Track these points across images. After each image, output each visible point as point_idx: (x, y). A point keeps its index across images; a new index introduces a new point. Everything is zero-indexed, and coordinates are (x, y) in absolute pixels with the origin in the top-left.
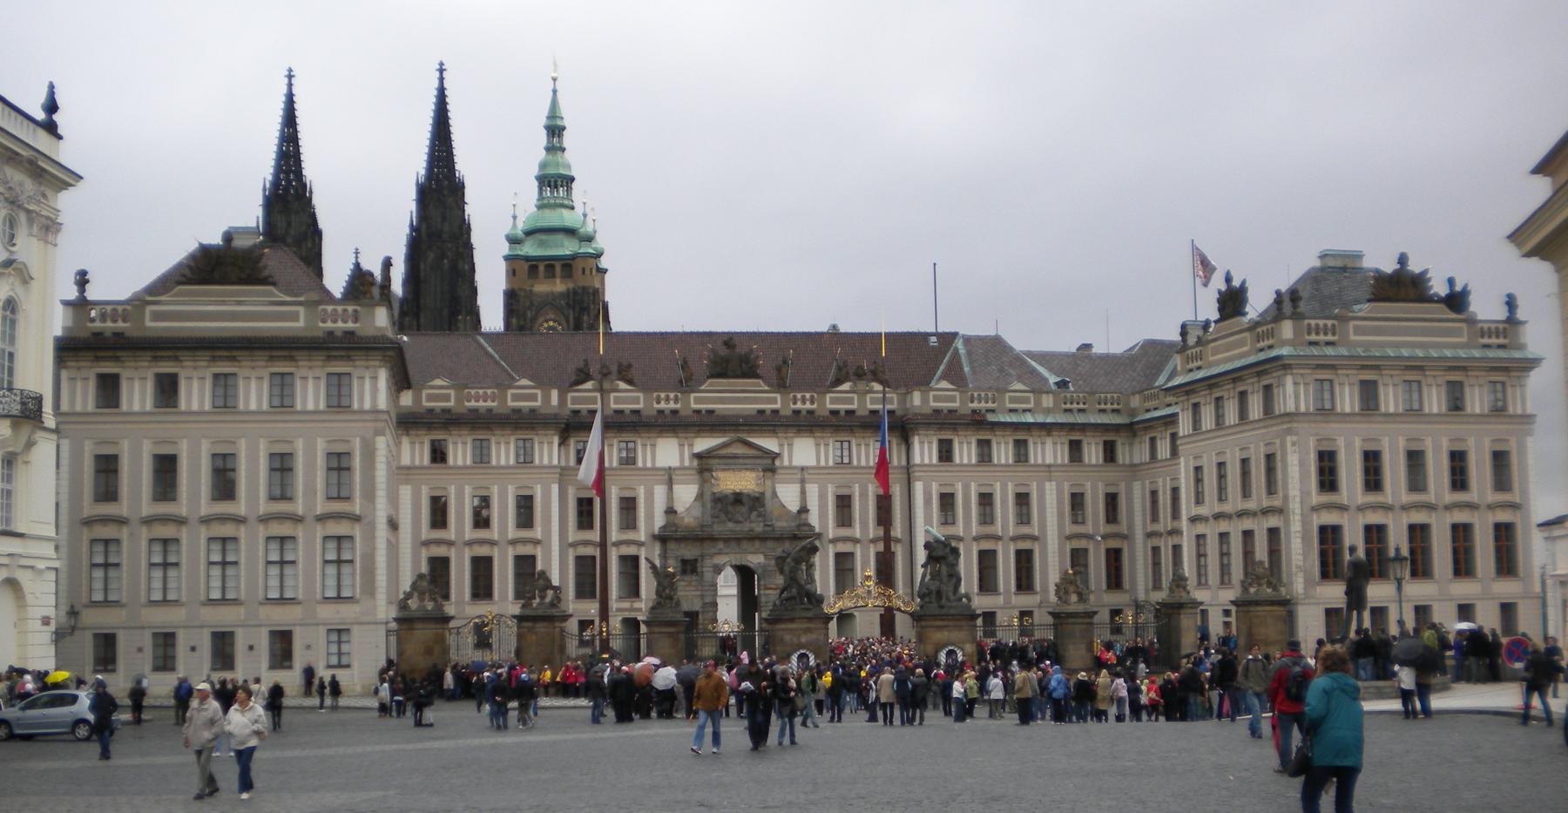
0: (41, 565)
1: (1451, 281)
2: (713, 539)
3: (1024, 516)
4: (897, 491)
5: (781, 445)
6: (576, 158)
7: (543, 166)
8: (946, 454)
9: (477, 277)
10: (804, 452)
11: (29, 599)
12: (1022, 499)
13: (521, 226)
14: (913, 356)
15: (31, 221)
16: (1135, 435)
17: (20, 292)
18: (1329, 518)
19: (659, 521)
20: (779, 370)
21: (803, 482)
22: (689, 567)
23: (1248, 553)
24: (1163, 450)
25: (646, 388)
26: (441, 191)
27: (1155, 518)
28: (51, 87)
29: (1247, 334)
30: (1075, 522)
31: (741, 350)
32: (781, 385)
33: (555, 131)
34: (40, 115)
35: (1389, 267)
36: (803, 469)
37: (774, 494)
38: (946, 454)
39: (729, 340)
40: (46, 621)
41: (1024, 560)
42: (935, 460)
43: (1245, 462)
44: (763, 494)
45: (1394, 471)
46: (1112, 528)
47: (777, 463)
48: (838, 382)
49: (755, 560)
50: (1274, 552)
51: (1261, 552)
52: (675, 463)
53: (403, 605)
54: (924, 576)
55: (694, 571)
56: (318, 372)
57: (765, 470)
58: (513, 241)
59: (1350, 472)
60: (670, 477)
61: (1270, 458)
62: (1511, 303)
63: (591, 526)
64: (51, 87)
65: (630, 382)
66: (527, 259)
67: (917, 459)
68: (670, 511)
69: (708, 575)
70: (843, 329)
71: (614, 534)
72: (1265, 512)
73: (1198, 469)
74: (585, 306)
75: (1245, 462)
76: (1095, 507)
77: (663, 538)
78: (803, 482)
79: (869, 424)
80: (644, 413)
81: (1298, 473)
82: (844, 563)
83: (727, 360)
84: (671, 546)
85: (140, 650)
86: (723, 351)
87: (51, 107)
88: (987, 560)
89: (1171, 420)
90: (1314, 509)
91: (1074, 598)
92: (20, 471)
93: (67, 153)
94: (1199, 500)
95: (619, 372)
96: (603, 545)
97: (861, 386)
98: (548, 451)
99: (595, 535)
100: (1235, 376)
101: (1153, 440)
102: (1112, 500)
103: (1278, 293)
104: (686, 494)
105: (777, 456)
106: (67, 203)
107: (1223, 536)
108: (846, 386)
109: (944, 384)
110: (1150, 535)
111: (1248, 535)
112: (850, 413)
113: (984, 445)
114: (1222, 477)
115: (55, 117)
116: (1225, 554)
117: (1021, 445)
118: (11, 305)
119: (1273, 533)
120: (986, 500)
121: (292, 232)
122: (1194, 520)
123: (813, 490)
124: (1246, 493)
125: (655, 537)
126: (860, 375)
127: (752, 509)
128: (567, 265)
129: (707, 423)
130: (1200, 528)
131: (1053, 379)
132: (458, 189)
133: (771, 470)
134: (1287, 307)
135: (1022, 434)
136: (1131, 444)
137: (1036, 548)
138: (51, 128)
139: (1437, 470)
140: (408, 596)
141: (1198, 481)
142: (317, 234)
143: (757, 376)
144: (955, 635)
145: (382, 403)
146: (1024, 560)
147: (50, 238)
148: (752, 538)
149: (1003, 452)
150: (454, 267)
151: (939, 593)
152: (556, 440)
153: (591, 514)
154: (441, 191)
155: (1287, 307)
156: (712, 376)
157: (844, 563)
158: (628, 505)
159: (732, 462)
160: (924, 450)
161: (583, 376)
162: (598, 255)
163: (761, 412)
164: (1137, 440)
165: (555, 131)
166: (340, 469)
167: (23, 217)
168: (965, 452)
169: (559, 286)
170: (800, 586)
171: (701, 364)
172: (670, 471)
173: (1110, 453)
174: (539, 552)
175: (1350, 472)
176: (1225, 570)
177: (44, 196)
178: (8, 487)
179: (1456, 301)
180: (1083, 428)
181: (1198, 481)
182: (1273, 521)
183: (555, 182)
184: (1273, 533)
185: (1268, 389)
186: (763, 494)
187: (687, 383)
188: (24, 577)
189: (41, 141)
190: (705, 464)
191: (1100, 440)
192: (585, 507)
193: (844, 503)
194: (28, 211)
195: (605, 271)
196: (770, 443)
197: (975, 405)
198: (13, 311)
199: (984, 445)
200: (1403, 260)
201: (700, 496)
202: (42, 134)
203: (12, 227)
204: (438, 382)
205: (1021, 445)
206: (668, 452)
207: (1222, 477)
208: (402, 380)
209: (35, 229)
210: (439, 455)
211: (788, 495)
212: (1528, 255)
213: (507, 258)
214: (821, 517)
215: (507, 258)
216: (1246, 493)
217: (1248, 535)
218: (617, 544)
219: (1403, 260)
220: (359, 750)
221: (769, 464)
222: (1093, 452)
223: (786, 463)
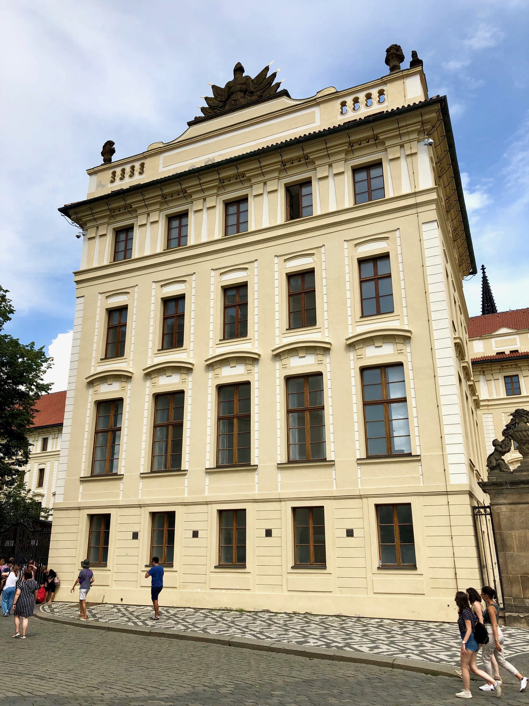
53: (495, 463)
140: (500, 448)
166: (377, 279)
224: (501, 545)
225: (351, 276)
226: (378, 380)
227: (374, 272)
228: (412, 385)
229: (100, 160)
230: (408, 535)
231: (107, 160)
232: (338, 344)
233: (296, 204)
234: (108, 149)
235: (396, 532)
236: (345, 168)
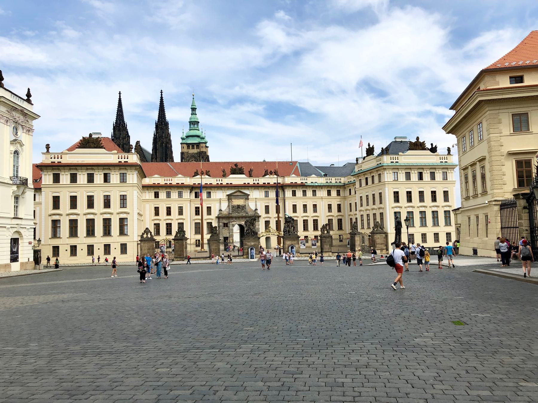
0: (28, 227)
1: (432, 144)
2: (232, 217)
3: (315, 211)
4: (281, 204)
6: (200, 116)
7: (190, 119)
8: (294, 194)
9: (173, 149)
10: (255, 194)
11: (24, 237)
12: (315, 206)
13: (185, 135)
14: (286, 168)
15: (23, 129)
17: (19, 149)
18: (397, 210)
20: (249, 172)
21: (256, 202)
22: (226, 225)
23: (375, 219)
24: (353, 192)
25: (214, 176)
26: (162, 125)
27: (351, 211)
28: (29, 89)
30: (329, 212)
31: (239, 167)
32: (250, 176)
33: (194, 109)
34: (26, 98)
35: (414, 140)
37: (248, 205)
38: (294, 194)
39: (236, 164)
40: (30, 243)
41: (315, 222)
42: (291, 196)
43: (374, 195)
44: (245, 205)
45: (415, 196)
46: (340, 214)
48: (265, 175)
49: (243, 223)
50: (382, 219)
51: (378, 219)
53: (142, 236)
54: (285, 227)
55: (227, 226)
56: (117, 173)
58: (183, 139)
59: (403, 197)
61: (380, 194)
62: (449, 150)
63: (199, 214)
64: (29, 89)
65: (209, 176)
66: (187, 144)
67: (286, 196)
68: (220, 210)
69: (231, 227)
71: (205, 216)
72: (380, 208)
73: (361, 197)
74: (203, 156)
75: (374, 195)
76: (335, 208)
77: (218, 218)
78: (256, 202)
81: (389, 197)
82: (267, 223)
83: (235, 170)
84: (221, 220)
85: (66, 250)
86: (234, 167)
87: (29, 95)
88: (305, 222)
89: (354, 184)
90: (393, 208)
91: (326, 232)
92: (21, 200)
93: (34, 109)
94: (362, 206)
96: (202, 219)
97: (271, 176)
98: (186, 194)
99: (200, 217)
100: (370, 171)
101: (350, 190)
102: (339, 206)
103: (382, 148)
104: (225, 206)
106: (35, 123)
108: (268, 176)
109: (293, 175)
110: (350, 215)
111: (374, 215)
112: (269, 183)
113: (304, 193)
114: (367, 199)
115: (30, 98)
116: (368, 220)
117: (314, 193)
118: (16, 153)
119: (382, 214)
120: (305, 206)
121: (121, 136)
122: (360, 211)
123: (258, 204)
124: (374, 204)
126: (271, 173)
127: (243, 209)
128: (198, 145)
129: (229, 186)
130: (355, 213)
131: (323, 174)
132: (166, 124)
133: (248, 199)
134: (385, 152)
135: (315, 188)
137: (318, 219)
138: (28, 101)
139: (428, 196)
140: (143, 234)
141: (361, 200)
142: (129, 137)
143: (243, 174)
144: (293, 242)
145: (135, 181)
146: (315, 222)
147: (30, 133)
148: (243, 217)
149: (309, 193)
150: (166, 146)
151: (289, 231)
152: (189, 191)
153: (199, 211)
154: (162, 125)
155: (385, 152)
156: (232, 174)
157: (267, 223)
158: (209, 209)
159: (237, 197)
160: (288, 193)
161: (196, 174)
162: (206, 143)
165: (194, 109)
167: (20, 127)
168: (299, 193)
169: (195, 151)
170: (251, 230)
171: (228, 171)
173: (338, 193)
174: (184, 222)
175: (403, 197)
176: (369, 224)
177: (27, 121)
178: (16, 205)
179: (434, 150)
180: (331, 186)
181: (361, 200)
182: (381, 211)
183: (194, 123)
184: (382, 214)
185: (380, 175)
186: (245, 205)
187: (224, 176)
188: (22, 231)
189: (25, 105)
190: (230, 197)
192: (197, 209)
193: (267, 208)
194: (22, 126)
195: (208, 147)
196: (247, 192)
197: (302, 181)
198: (18, 154)
199: (304, 193)
200: (418, 138)
201: (229, 206)
202: (25, 103)
203: (16, 130)
204: (156, 176)
205: (314, 193)
206: (221, 195)
207: (367, 199)
208: (143, 175)
209: (25, 131)
210: (157, 195)
211: (252, 205)
212: (448, 133)
213: (181, 144)
214: (261, 212)
215: (181, 144)
216: (374, 204)
217: (374, 215)
219: (418, 138)
220: (19, 285)
221: (247, 197)
222: (334, 193)
224: (141, 250)
225: (118, 199)
226: (122, 222)
227: (123, 199)
228: (129, 222)
229: (45, 150)
230: (126, 248)
231: (48, 151)
232: (115, 213)
233: (106, 179)
234: (48, 147)
235: (124, 248)
236: (118, 173)
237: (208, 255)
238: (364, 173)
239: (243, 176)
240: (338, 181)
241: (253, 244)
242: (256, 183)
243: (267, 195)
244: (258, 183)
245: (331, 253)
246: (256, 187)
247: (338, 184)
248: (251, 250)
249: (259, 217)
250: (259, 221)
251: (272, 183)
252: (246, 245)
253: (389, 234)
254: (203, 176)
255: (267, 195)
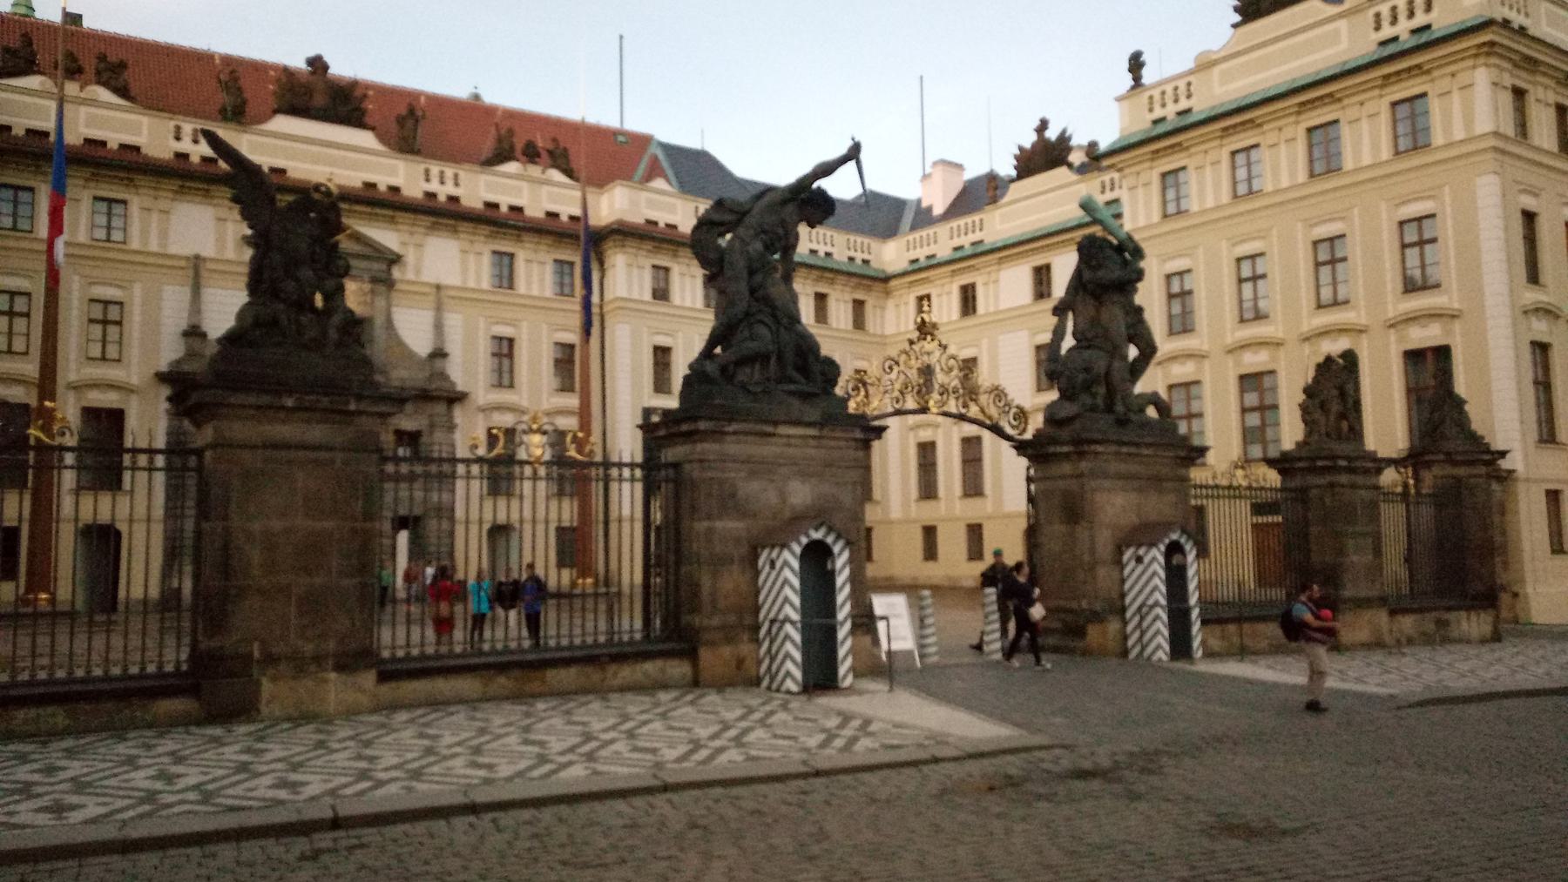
5: (404, 244)
10: (439, 260)
16: (888, 293)
19: (169, 351)
20: (401, 121)
21: (439, 309)
29: (1342, 24)
36: (438, 287)
42: (648, 296)
47: (396, 273)
52: (208, 251)
57: (375, 280)
60: (196, 270)
68: (194, 333)
70: (490, 97)
71: (71, 368)
78: (439, 309)
79: (550, 230)
80: (144, 151)
95: (98, 73)
97: (534, 171)
105: (395, 260)
107: (1249, 381)
108: (512, 167)
123: (454, 321)
125: (162, 378)
126: (531, 154)
136: (883, 308)
158: (108, 316)
163: (371, 186)
164: (891, 303)
172: (197, 262)
191: (849, 296)
193: (505, 350)
196: (386, 236)
214: (468, 369)
218: (76, 388)
223: (410, 276)
237: (174, 655)
238: (1237, 117)
239: (365, 138)
240: (859, 256)
241: (800, 494)
242: (443, 191)
243: (505, 275)
244: (453, 199)
245: (1382, 617)
246: (444, 215)
247: (857, 267)
248: (817, 556)
249: (455, 398)
250: (451, 428)
251: (535, 211)
252: (730, 503)
253: (1521, 488)
254: (71, 88)
255: (505, 275)
